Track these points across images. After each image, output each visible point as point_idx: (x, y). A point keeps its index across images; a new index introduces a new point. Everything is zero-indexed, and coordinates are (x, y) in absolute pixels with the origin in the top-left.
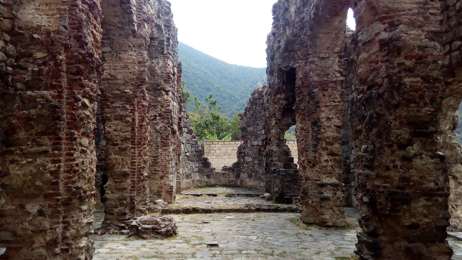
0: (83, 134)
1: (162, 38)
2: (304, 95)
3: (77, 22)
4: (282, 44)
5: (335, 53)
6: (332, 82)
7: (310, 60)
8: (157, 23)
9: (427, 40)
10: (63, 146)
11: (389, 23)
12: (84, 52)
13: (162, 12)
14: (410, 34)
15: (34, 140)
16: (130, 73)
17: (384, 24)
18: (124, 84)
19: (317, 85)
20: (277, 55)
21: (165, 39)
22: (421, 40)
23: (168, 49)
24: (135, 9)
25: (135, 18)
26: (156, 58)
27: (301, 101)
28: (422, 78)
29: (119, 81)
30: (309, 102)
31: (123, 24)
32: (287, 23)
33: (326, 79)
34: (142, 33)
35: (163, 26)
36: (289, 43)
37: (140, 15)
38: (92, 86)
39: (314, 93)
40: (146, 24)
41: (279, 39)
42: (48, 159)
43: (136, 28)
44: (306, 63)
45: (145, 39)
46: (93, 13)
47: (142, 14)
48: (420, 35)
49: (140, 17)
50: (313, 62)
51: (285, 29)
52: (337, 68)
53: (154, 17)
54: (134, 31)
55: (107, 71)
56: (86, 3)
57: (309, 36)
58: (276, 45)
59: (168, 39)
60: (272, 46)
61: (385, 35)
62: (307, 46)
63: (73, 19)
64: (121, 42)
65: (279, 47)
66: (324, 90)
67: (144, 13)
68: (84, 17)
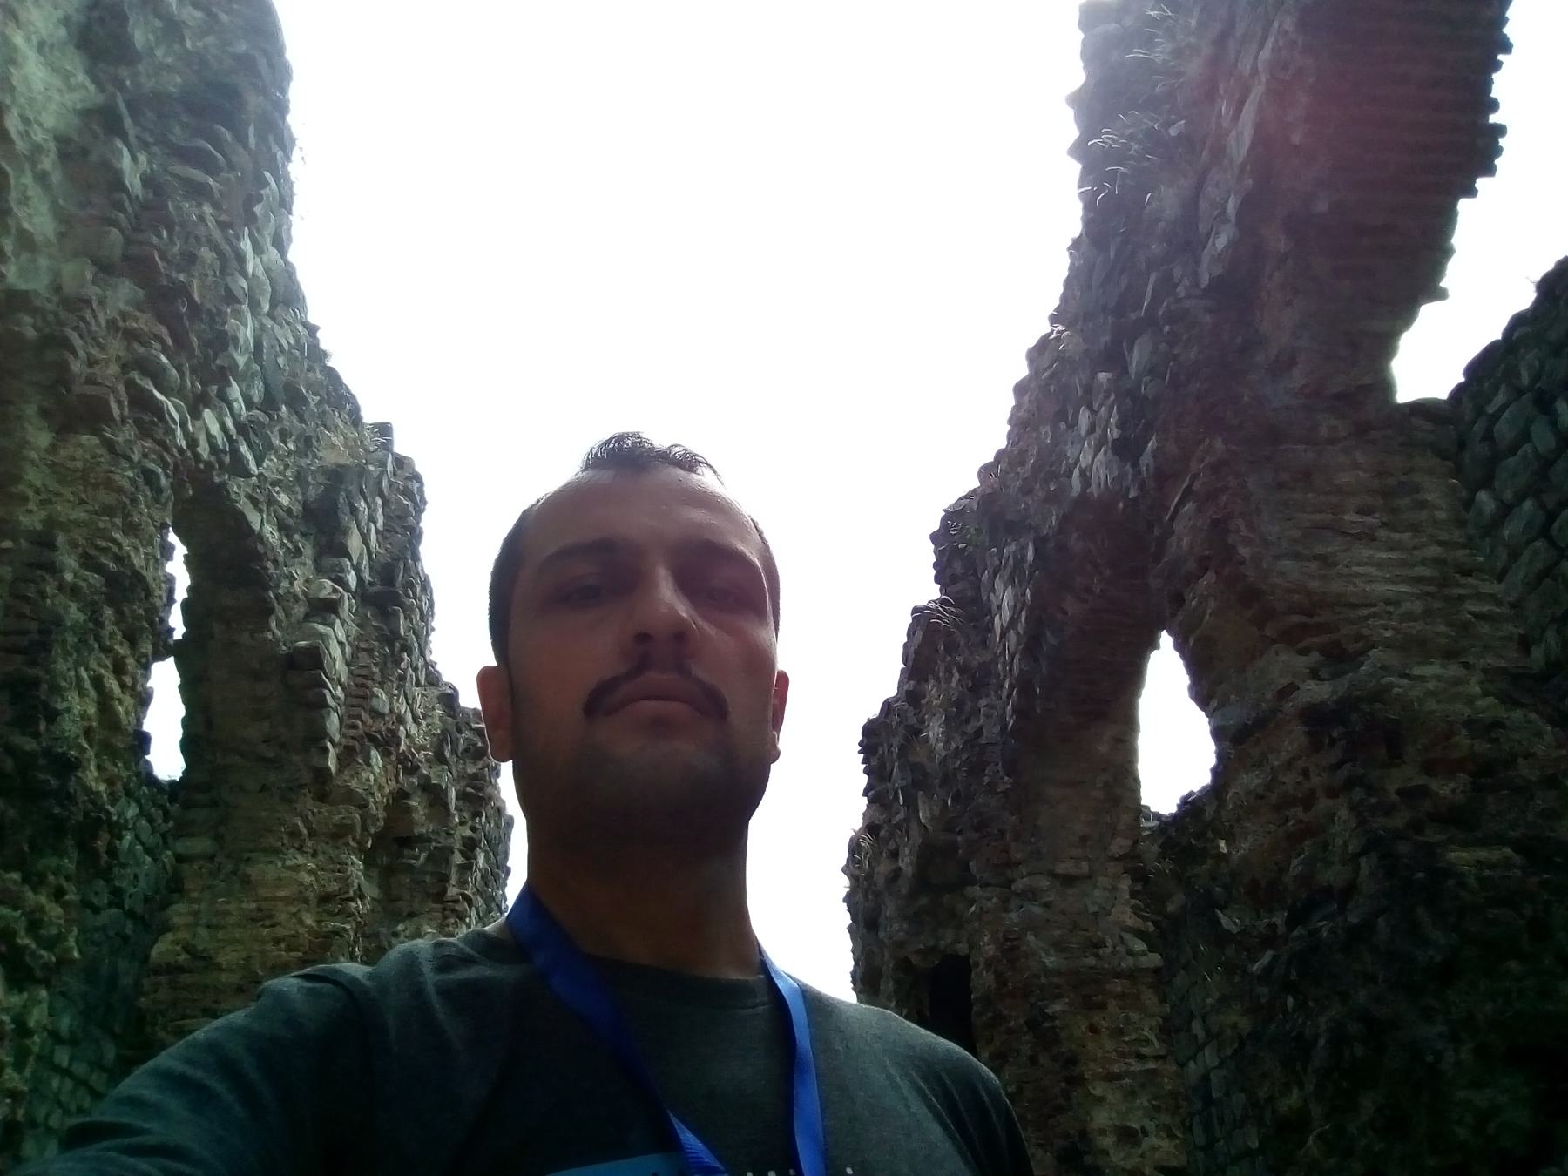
1: (443, 842)
2: (1010, 1031)
3: (34, 626)
4: (906, 863)
5: (1113, 859)
6: (1119, 975)
7: (1019, 885)
8: (428, 778)
9: (1491, 699)
11: (1325, 651)
12: (29, 745)
13: (455, 743)
14: (1422, 678)
16: (277, 941)
17: (1304, 652)
18: (240, 990)
19: (1058, 986)
20: (890, 909)
21: (458, 846)
22: (1470, 700)
23: (463, 883)
24: (339, 692)
25: (333, 723)
26: (411, 915)
28: (1517, 846)
29: (224, 977)
30: (1033, 1060)
31: (283, 746)
32: (919, 781)
33: (1091, 961)
34: (354, 783)
35: (453, 794)
36: (929, 854)
37: (359, 717)
38: (41, 909)
39: (1053, 1018)
40: (374, 753)
41: (892, 846)
43: (332, 764)
44: (1005, 901)
45: (363, 806)
46: (119, 613)
47: (365, 716)
48: (1458, 682)
49: (355, 727)
50: (1031, 894)
51: (911, 804)
52: (1130, 920)
53: (421, 756)
54: (322, 774)
55: (183, 935)
56: (99, 569)
57: (1005, 792)
58: (884, 868)
59: (470, 846)
60: (869, 876)
61: (1318, 692)
62: (1002, 833)
63: (21, 616)
64: (264, 814)
65: (897, 874)
66: (1090, 1005)
67: (377, 714)
68: (74, 613)
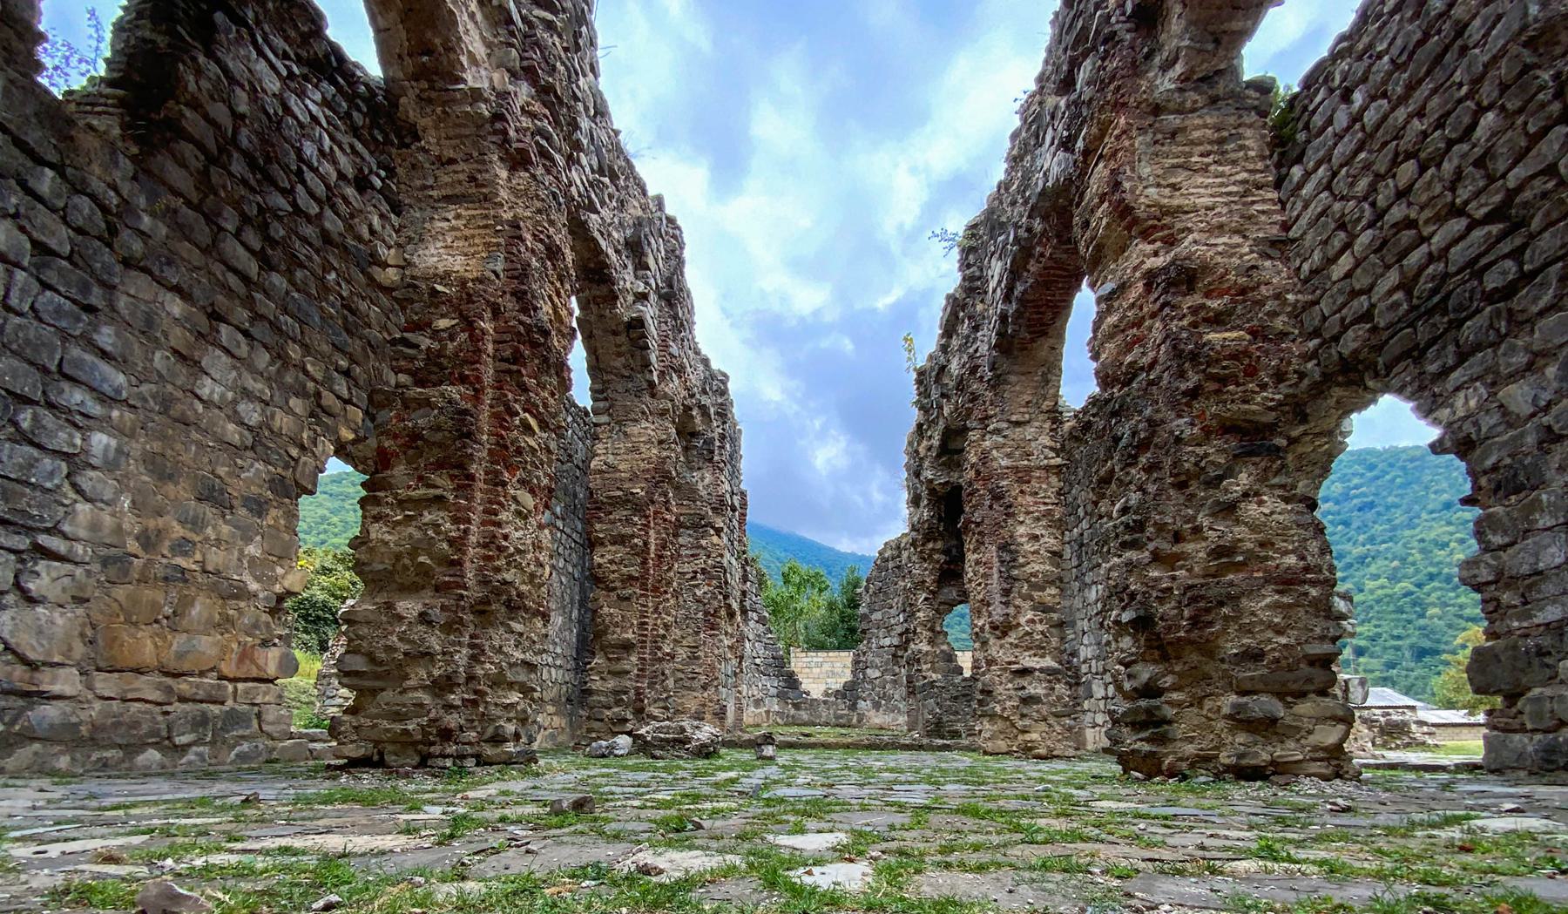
0: (522, 482)
10: (478, 495)
15: (421, 478)
27: (975, 507)
30: (991, 507)
42: (442, 514)
